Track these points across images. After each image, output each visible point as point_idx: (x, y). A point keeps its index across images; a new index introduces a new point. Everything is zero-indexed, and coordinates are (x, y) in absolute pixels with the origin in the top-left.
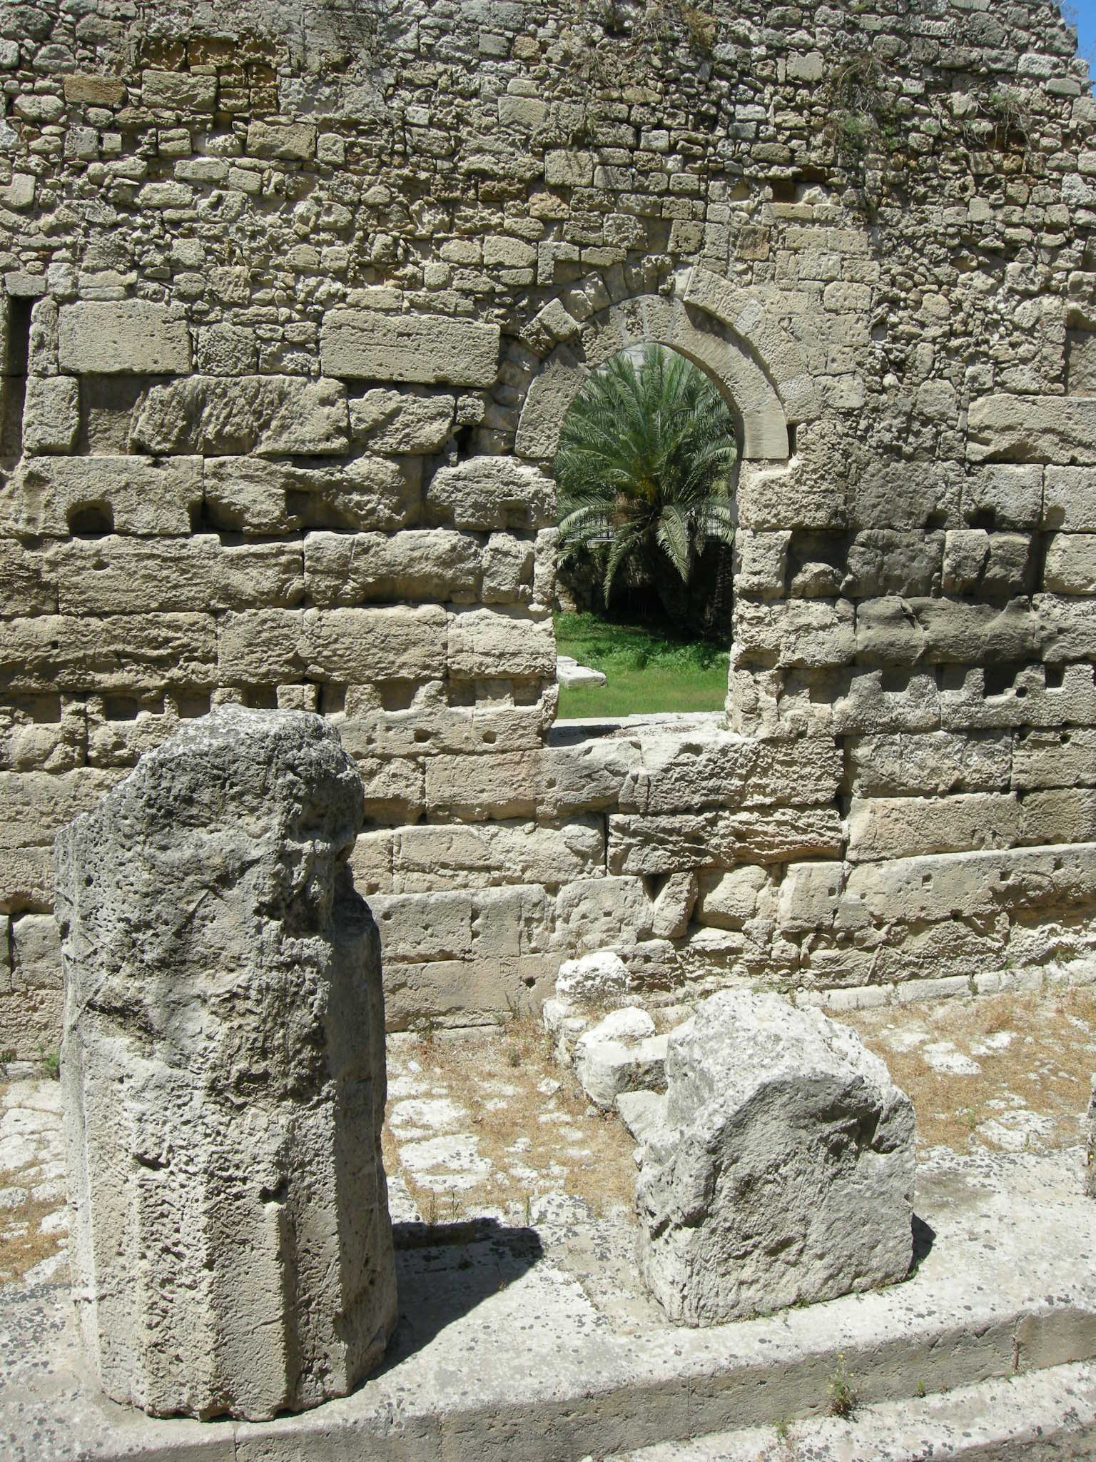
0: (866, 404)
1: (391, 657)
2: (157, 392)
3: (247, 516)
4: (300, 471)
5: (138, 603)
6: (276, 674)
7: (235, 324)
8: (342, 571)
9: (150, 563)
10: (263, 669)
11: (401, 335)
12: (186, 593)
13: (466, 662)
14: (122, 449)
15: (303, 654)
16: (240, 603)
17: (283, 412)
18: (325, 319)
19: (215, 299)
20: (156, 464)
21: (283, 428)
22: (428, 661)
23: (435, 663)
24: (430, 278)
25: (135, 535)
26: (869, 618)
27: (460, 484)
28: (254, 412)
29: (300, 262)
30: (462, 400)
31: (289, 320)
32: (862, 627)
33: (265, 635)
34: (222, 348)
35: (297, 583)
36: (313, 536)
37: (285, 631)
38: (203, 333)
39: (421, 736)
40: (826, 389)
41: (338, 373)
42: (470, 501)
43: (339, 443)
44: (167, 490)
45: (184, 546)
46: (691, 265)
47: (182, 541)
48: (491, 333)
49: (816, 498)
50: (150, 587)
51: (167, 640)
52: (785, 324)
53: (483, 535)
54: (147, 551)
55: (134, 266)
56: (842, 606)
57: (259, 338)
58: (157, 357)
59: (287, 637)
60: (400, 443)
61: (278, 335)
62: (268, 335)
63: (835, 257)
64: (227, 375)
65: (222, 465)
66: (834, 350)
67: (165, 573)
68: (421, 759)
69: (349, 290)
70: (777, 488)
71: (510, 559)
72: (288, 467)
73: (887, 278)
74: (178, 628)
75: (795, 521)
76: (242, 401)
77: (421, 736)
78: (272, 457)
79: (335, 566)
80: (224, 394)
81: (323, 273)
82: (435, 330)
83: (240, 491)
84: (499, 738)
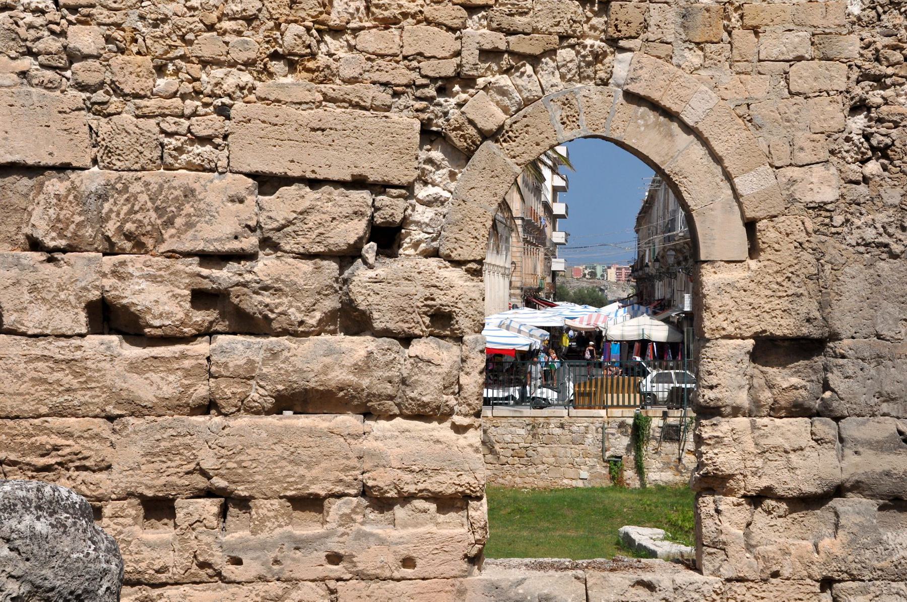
0: (842, 196)
1: (302, 471)
2: (55, 185)
3: (148, 317)
4: (205, 272)
5: (25, 407)
6: (173, 486)
7: (137, 117)
8: (247, 376)
9: (40, 365)
10: (163, 480)
11: (314, 130)
12: (80, 397)
13: (381, 479)
14: (14, 243)
15: (205, 466)
16: (139, 410)
17: (188, 209)
18: (233, 113)
19: (117, 91)
20: (50, 260)
21: (189, 225)
22: (342, 476)
23: (349, 479)
24: (347, 73)
25: (23, 334)
26: (856, 442)
27: (377, 287)
28: (157, 209)
29: (207, 53)
30: (382, 199)
31: (194, 114)
32: (848, 452)
33: (164, 445)
34: (120, 141)
35: (201, 391)
36: (222, 339)
37: (187, 440)
38: (103, 126)
39: (334, 558)
40: (793, 182)
41: (247, 169)
42: (387, 303)
43: (250, 242)
44: (61, 288)
45: (79, 348)
46: (630, 50)
47: (77, 342)
48: (410, 127)
49: (785, 303)
50: (40, 391)
51: (56, 448)
52: (743, 110)
53: (406, 340)
54: (38, 352)
55: (30, 52)
56: (825, 427)
57: (163, 131)
58: (50, 148)
59: (188, 447)
60: (313, 242)
61: (183, 129)
62: (173, 128)
63: (805, 34)
64: (129, 170)
65: (123, 263)
66: (802, 137)
67: (58, 375)
68: (332, 584)
69: (258, 84)
70: (734, 293)
71: (434, 369)
72: (193, 265)
73: (869, 54)
74: (70, 435)
75: (758, 328)
76: (144, 198)
77: (334, 558)
78: (172, 254)
79: (241, 372)
80: (126, 188)
81: (233, 64)
82: (351, 125)
83: (141, 291)
84: (419, 562)
